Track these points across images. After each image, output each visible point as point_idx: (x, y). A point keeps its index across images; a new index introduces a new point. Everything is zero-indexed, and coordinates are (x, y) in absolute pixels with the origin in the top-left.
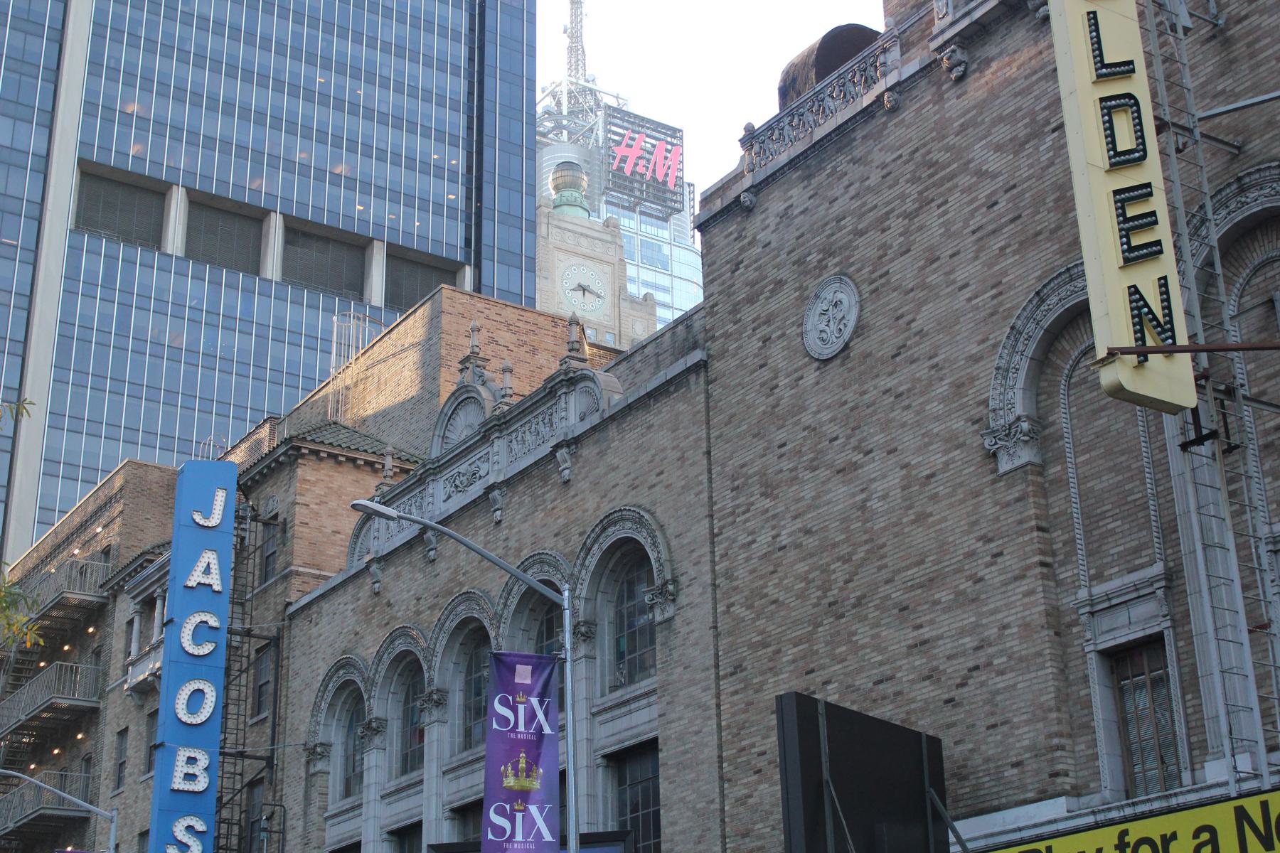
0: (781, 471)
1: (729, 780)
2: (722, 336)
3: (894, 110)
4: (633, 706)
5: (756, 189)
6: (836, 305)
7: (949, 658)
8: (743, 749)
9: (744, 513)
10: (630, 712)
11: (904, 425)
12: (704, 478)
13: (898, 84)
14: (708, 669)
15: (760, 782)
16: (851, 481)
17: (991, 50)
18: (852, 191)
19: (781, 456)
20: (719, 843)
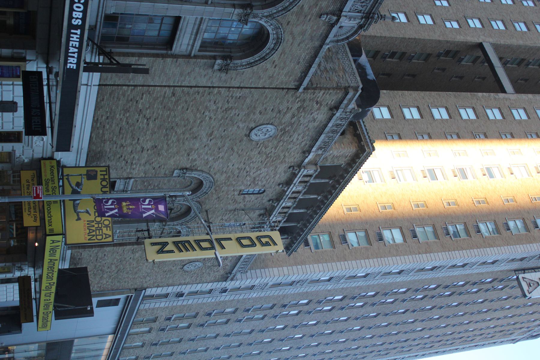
0: (230, 114)
1: (134, 89)
2: (300, 96)
3: (304, 152)
4: (193, 36)
5: (334, 115)
6: (266, 134)
7: (134, 157)
8: (143, 95)
9: (228, 100)
10: (191, 34)
11: (210, 150)
12: (254, 86)
13: (307, 157)
14: (182, 83)
15: (127, 101)
16: (207, 134)
17: (288, 174)
18: (295, 140)
19: (235, 114)
20: (112, 83)
